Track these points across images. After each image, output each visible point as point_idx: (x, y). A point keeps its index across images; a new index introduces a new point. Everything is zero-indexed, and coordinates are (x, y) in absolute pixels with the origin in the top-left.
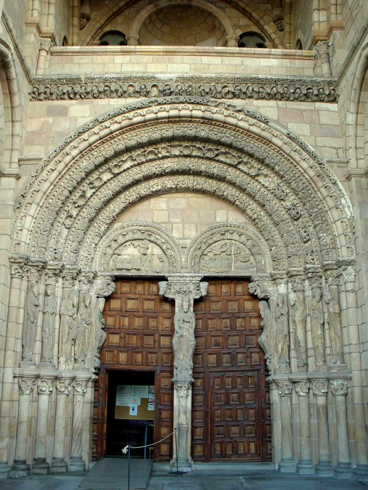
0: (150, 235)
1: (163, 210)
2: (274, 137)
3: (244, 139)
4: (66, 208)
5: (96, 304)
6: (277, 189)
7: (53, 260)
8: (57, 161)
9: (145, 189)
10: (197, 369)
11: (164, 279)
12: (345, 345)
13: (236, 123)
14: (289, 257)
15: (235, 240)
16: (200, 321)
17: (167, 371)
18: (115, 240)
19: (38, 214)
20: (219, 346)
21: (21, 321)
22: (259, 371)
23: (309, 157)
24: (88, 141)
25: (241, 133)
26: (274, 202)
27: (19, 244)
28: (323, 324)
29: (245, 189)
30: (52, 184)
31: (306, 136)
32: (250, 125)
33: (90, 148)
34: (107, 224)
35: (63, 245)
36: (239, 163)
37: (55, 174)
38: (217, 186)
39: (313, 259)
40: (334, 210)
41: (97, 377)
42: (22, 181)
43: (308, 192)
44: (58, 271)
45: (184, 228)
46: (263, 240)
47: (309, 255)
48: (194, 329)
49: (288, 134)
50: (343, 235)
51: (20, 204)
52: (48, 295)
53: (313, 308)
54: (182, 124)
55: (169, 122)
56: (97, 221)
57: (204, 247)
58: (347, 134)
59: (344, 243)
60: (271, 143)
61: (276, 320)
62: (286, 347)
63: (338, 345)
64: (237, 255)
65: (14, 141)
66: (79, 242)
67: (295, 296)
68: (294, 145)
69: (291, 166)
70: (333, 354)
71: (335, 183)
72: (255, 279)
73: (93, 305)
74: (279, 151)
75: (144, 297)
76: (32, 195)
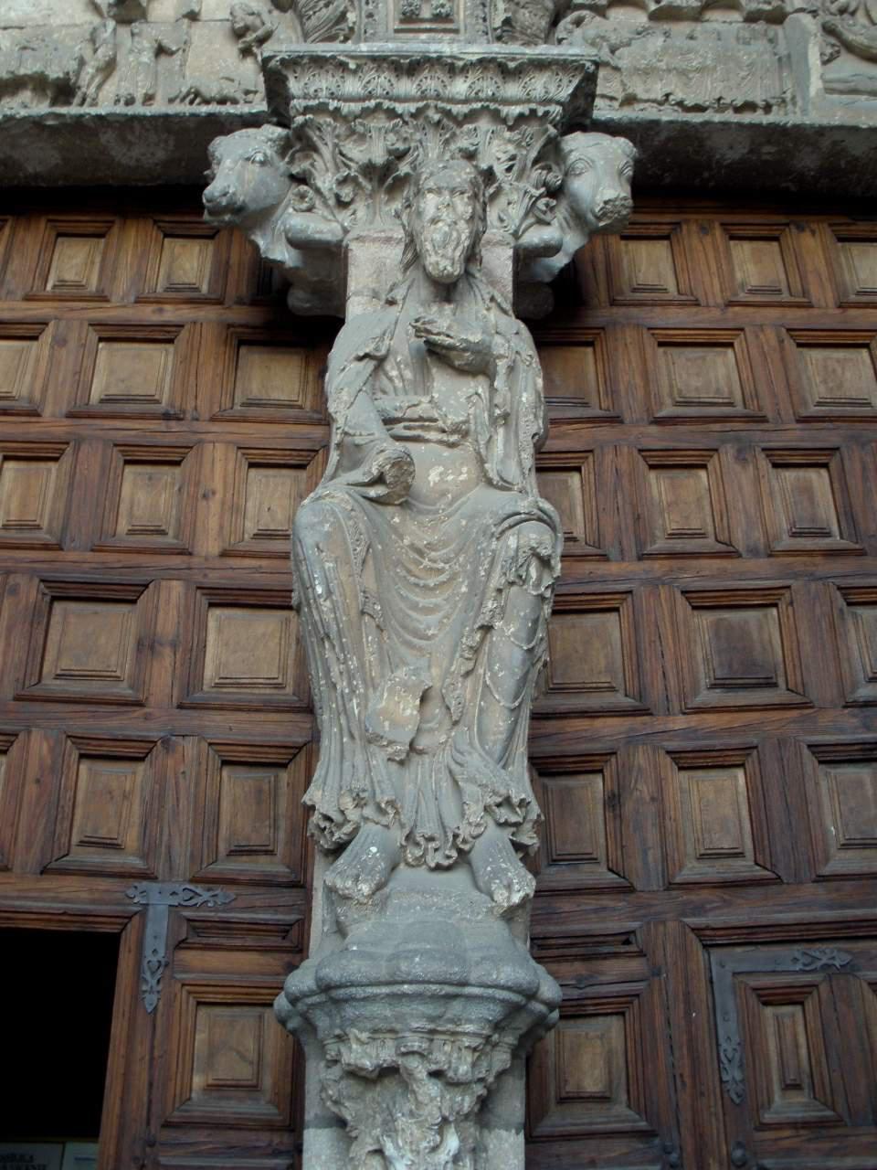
17: (254, 928)
20: (770, 684)
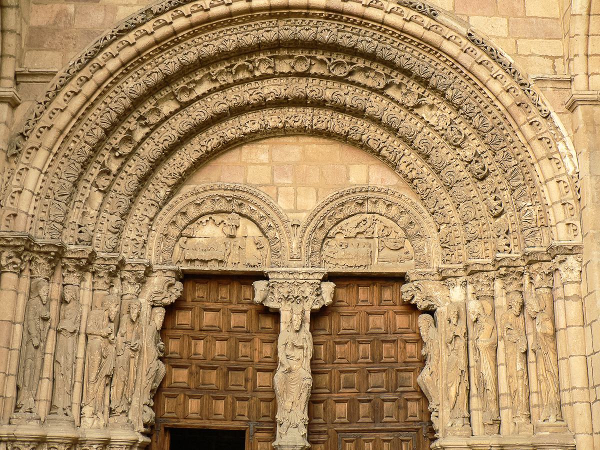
0: (240, 205)
1: (263, 164)
2: (445, 41)
3: (395, 45)
4: (100, 159)
5: (150, 318)
6: (449, 129)
7: (76, 244)
8: (82, 78)
9: (233, 130)
10: (316, 426)
11: (262, 276)
12: (565, 390)
13: (382, 17)
14: (469, 241)
15: (381, 215)
16: (322, 346)
18: (184, 213)
19: (50, 166)
20: (353, 388)
21: (16, 345)
22: (420, 431)
23: (504, 74)
24: (136, 45)
25: (391, 35)
26: (445, 151)
27: (15, 215)
28: (526, 353)
29: (398, 130)
30: (74, 116)
31: (501, 37)
32: (405, 20)
33: (139, 59)
34: (169, 186)
35: (94, 220)
36: (387, 86)
37: (78, 101)
38: (351, 126)
39: (508, 245)
40: (547, 160)
41: (148, 440)
42: (21, 111)
43: (502, 133)
44: (84, 261)
45: (296, 194)
46: (426, 214)
47: (502, 237)
48: (311, 360)
49: (470, 35)
50: (560, 204)
51: (17, 148)
52: (67, 303)
53: (509, 326)
54: (293, 20)
55: (271, 16)
56: (154, 181)
57: (328, 224)
58: (572, 33)
59: (561, 217)
60: (441, 50)
61: (447, 346)
62: (463, 392)
63: (552, 389)
64: (382, 239)
65: (6, 41)
66: (122, 215)
67: (479, 305)
68: (479, 52)
69: (473, 89)
70: (543, 405)
71: (547, 117)
72: (413, 278)
73: (144, 318)
74: (453, 64)
75: (230, 307)
76: (39, 134)
